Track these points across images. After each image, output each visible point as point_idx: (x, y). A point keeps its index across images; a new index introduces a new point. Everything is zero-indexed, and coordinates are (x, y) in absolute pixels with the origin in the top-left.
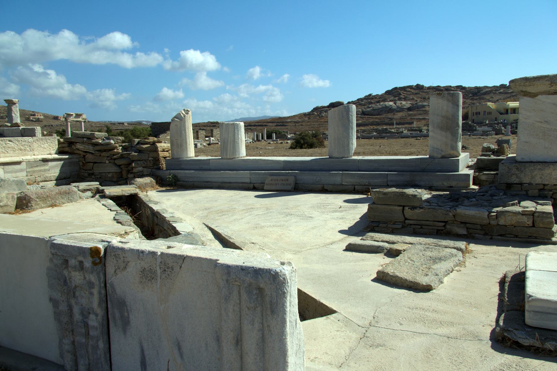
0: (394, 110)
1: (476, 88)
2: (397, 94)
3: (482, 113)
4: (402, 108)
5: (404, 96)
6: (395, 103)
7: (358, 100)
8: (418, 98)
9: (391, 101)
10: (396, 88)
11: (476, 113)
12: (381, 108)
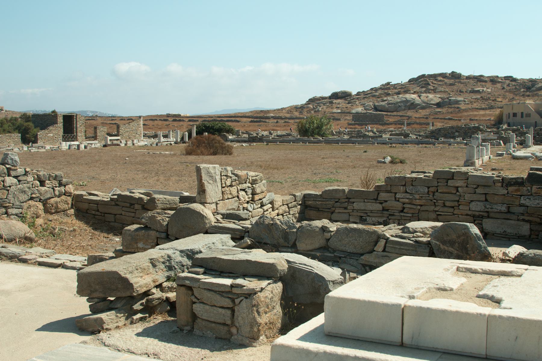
0: (419, 105)
2: (425, 84)
3: (519, 115)
4: (428, 104)
5: (434, 87)
6: (419, 96)
7: (372, 89)
9: (414, 93)
10: (423, 76)
12: (400, 102)
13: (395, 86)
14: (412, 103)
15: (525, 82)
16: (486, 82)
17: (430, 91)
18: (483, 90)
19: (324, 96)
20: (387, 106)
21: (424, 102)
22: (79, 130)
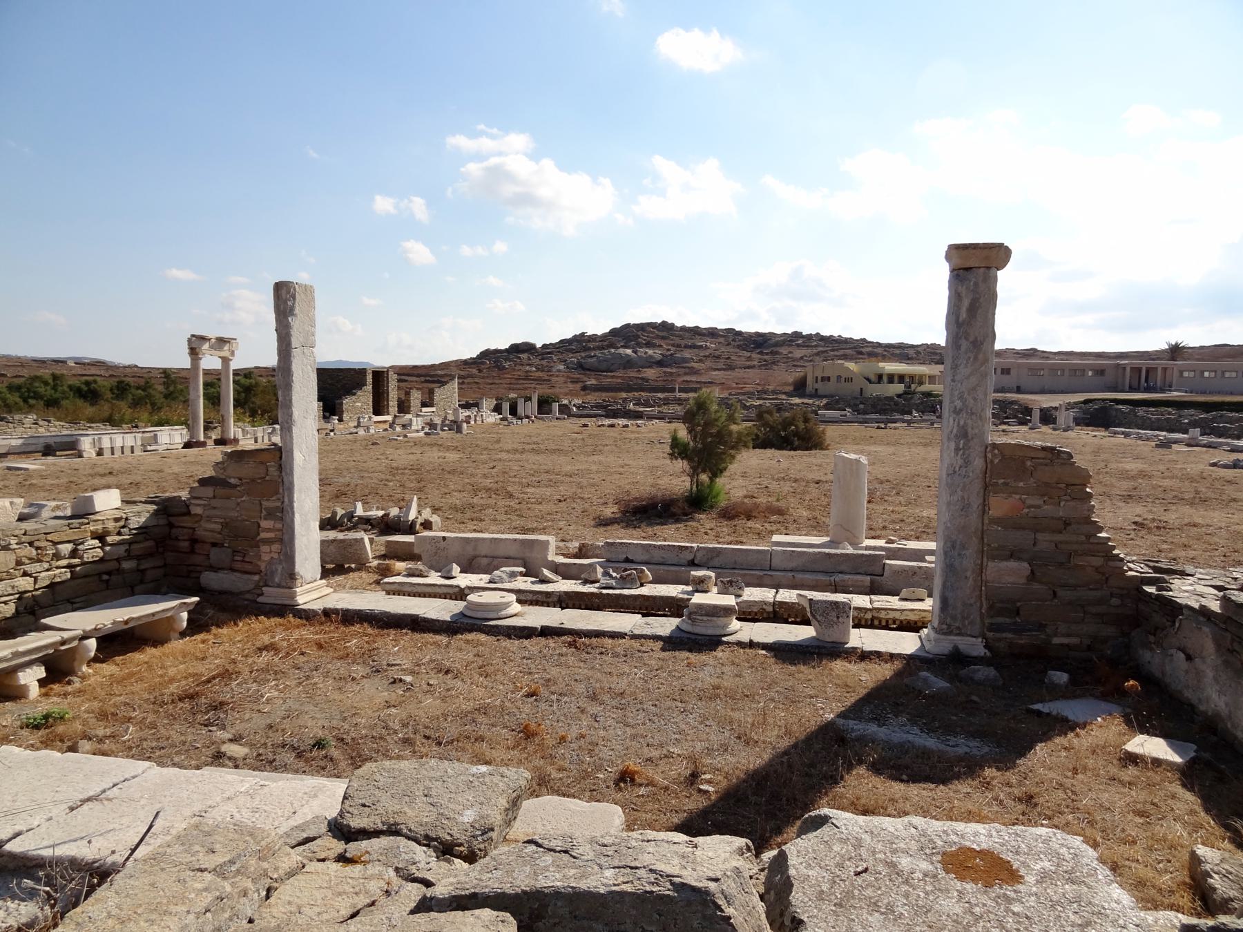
1: (757, 334)
3: (833, 379)
6: (635, 352)
8: (668, 345)
9: (625, 347)
10: (627, 326)
11: (822, 378)
13: (593, 338)
15: (752, 337)
22: (391, 395)
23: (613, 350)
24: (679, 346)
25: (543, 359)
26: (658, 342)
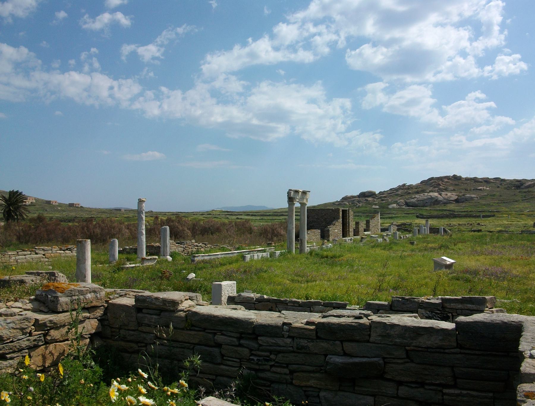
0: (441, 201)
2: (436, 185)
4: (448, 200)
5: (444, 187)
6: (440, 194)
10: (432, 179)
12: (426, 199)
13: (410, 187)
14: (436, 200)
16: (481, 182)
17: (443, 190)
18: (484, 189)
19: (353, 195)
20: (416, 203)
21: (445, 199)
23: (426, 194)
24: (466, 190)
25: (383, 200)
26: (451, 188)
